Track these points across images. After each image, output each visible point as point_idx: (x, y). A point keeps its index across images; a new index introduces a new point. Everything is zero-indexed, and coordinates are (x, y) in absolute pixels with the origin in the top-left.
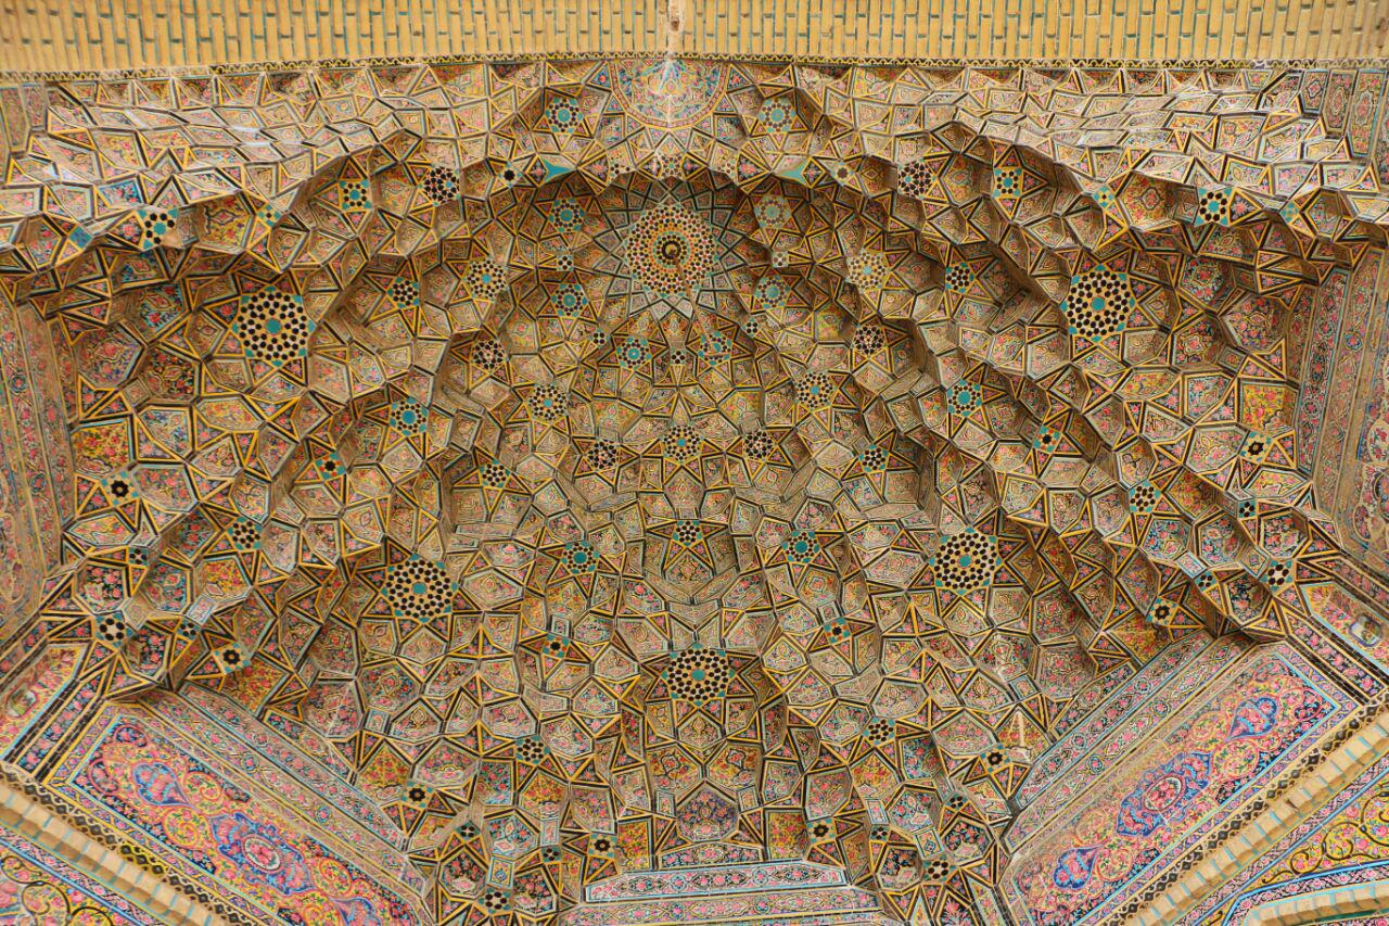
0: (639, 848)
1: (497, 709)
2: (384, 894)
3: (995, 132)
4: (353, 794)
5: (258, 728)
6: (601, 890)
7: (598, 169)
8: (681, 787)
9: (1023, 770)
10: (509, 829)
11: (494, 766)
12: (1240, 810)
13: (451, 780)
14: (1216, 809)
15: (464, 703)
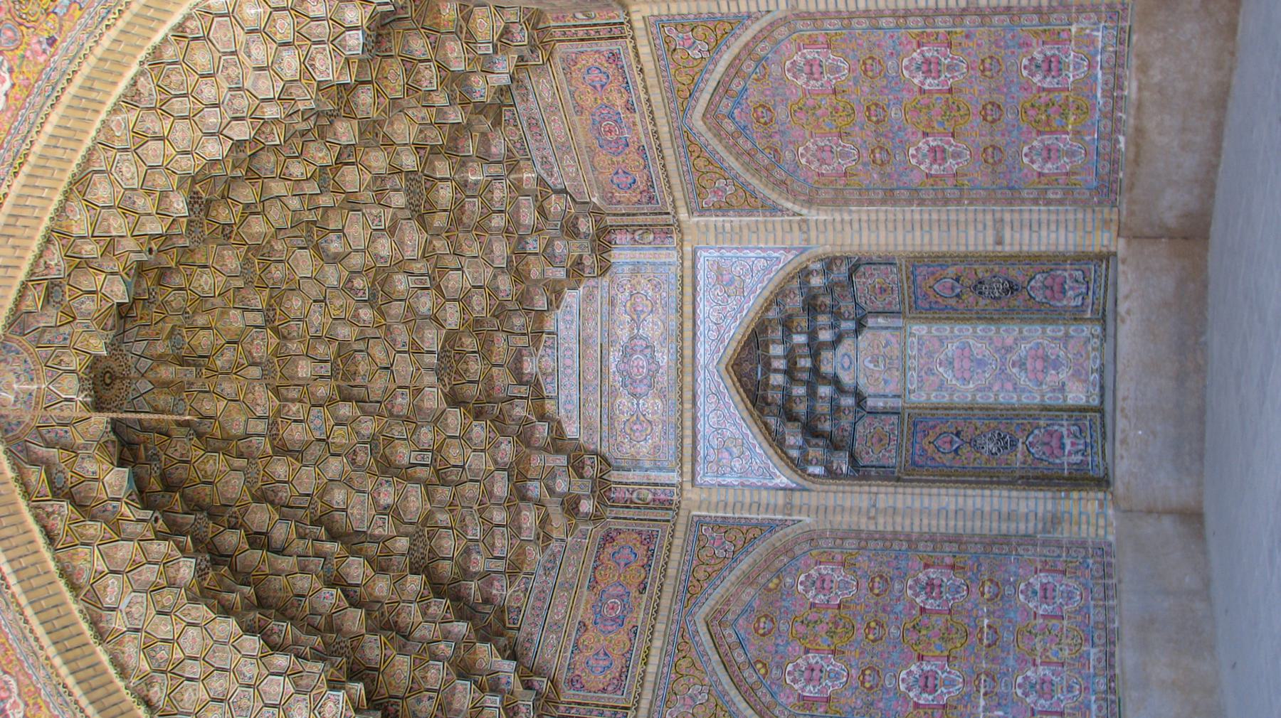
0: (542, 406)
1: (491, 494)
2: (602, 547)
3: (214, 149)
4: (541, 572)
5: (526, 628)
6: (571, 430)
7: (111, 449)
8: (503, 378)
9: (540, 181)
10: (550, 483)
11: (519, 494)
12: (645, 107)
13: (529, 518)
14: (637, 116)
15: (486, 515)
